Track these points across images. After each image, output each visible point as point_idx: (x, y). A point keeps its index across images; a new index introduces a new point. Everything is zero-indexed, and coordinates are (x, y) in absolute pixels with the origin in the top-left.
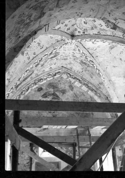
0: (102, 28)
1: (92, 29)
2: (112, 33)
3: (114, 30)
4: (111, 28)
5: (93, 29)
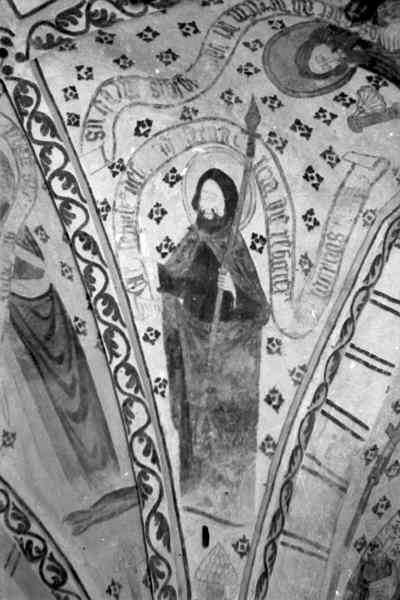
0: (143, 221)
1: (117, 168)
2: (141, 277)
3: (155, 282)
4: (163, 273)
5: (115, 174)
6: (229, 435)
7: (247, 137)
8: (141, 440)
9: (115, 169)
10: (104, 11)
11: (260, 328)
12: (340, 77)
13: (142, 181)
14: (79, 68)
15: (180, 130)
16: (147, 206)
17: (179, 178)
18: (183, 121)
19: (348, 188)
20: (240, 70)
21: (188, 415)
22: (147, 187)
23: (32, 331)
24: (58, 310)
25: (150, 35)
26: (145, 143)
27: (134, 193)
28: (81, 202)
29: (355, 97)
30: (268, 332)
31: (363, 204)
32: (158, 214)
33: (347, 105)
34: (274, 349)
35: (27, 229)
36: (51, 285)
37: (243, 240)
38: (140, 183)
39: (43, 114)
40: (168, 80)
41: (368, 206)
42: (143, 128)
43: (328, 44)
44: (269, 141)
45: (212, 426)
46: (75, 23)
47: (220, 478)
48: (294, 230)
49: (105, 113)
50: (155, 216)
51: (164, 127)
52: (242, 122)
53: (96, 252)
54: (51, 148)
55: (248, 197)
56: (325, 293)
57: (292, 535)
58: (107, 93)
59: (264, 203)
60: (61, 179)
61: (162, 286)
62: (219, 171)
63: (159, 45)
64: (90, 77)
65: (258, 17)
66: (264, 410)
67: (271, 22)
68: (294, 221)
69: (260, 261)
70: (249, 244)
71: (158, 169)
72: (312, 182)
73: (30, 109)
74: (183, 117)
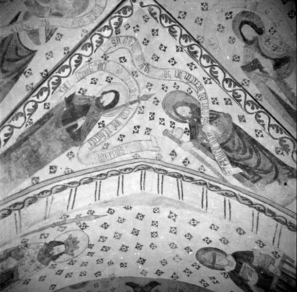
0: (89, 78)
1: (106, 57)
2: (67, 88)
3: (67, 96)
5: (102, 57)
6: (28, 162)
7: (137, 99)
8: (9, 129)
9: (104, 56)
10: (176, 32)
11: (73, 146)
12: (181, 119)
13: (103, 69)
14: (137, 26)
15: (127, 73)
16: (95, 75)
17: (110, 82)
18: (131, 73)
19: (141, 144)
20: (163, 85)
21: (24, 142)
22: (102, 72)
23: (6, 51)
24: (27, 58)
25: (163, 48)
26: (118, 63)
27: (98, 68)
28: (94, 50)
29: (175, 128)
30: (74, 149)
31: (139, 151)
32: (94, 82)
33: (171, 127)
34: (70, 156)
35: (56, 29)
36: (36, 51)
37: (99, 118)
38: (102, 68)
39: (122, 21)
40: (145, 61)
41: (139, 153)
42: (123, 59)
43: (191, 109)
44: (140, 107)
45: (26, 154)
46: (166, 22)
47: (10, 172)
48: (114, 135)
49: (123, 43)
50: (93, 81)
51: (126, 67)
52: (141, 95)
53: (76, 66)
54: (110, 29)
55: (115, 111)
56: (102, 160)
57: (20, 215)
58: (131, 41)
59: (116, 118)
60: (99, 38)
61: (67, 99)
62: (119, 95)
63: (160, 53)
64: (135, 31)
65: (190, 84)
66: (47, 168)
67: (190, 89)
68: (117, 132)
69: (96, 129)
70: (99, 122)
71: (110, 73)
72: (135, 130)
73: (122, 15)
74: (132, 72)
